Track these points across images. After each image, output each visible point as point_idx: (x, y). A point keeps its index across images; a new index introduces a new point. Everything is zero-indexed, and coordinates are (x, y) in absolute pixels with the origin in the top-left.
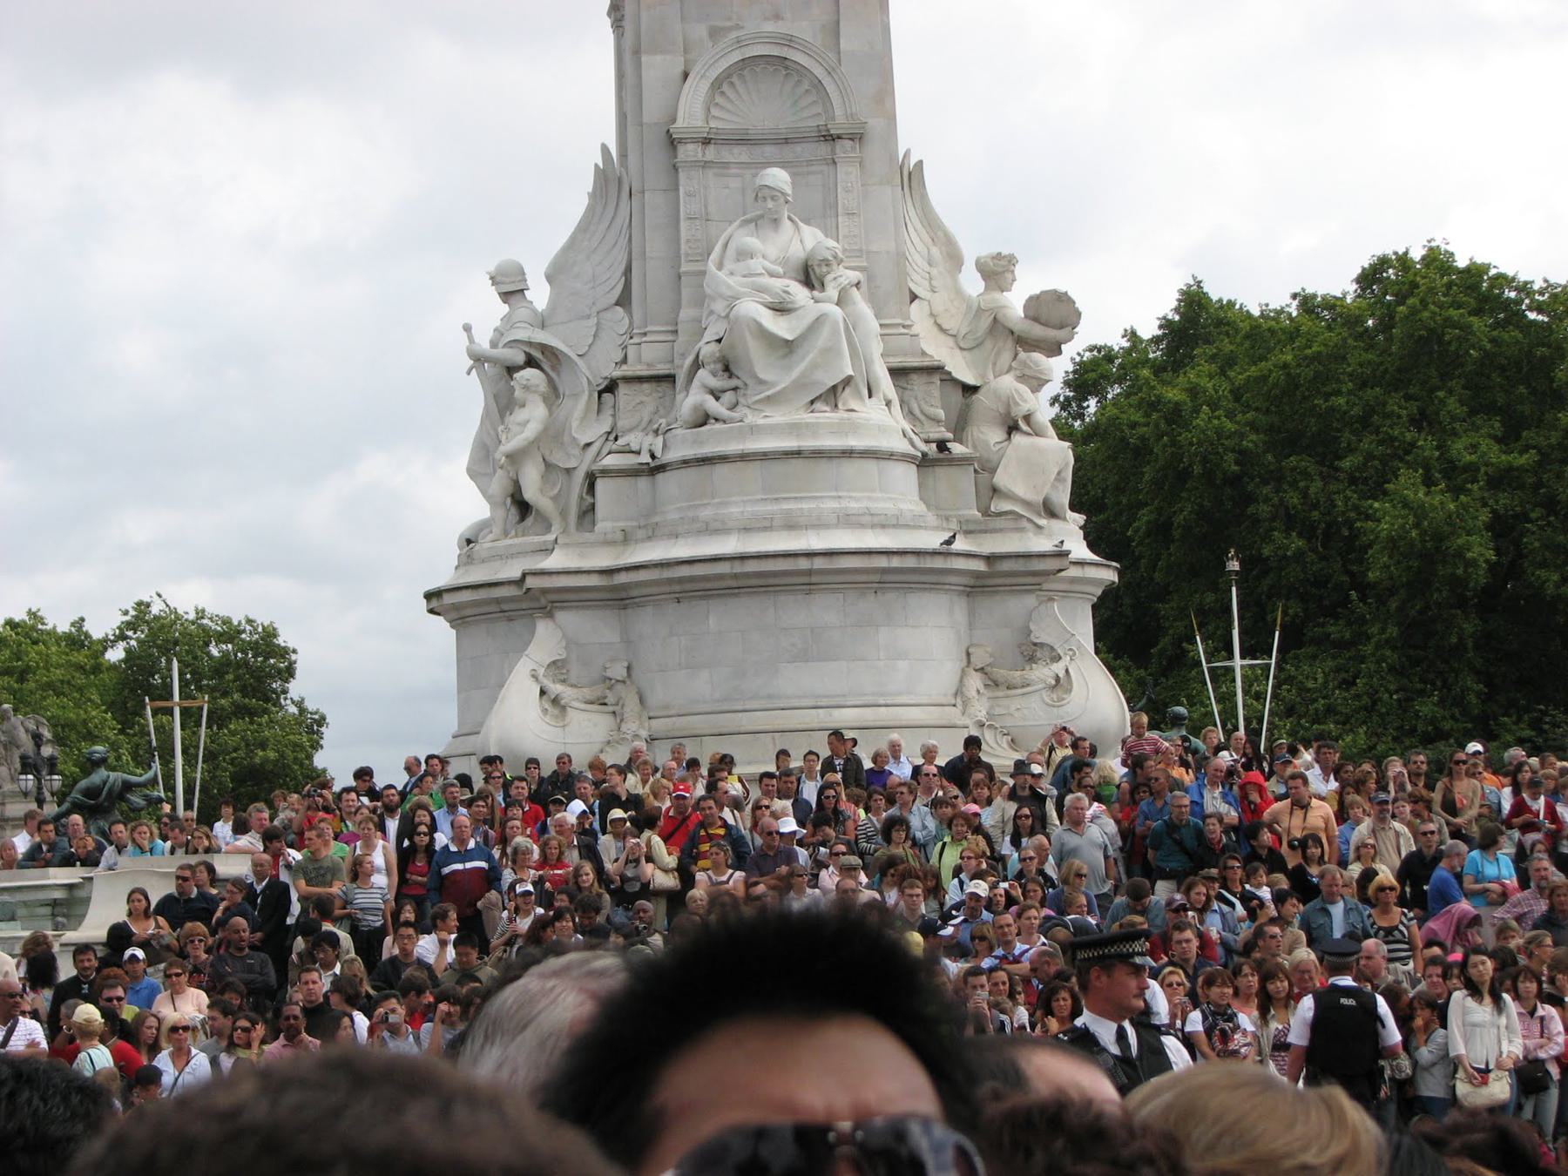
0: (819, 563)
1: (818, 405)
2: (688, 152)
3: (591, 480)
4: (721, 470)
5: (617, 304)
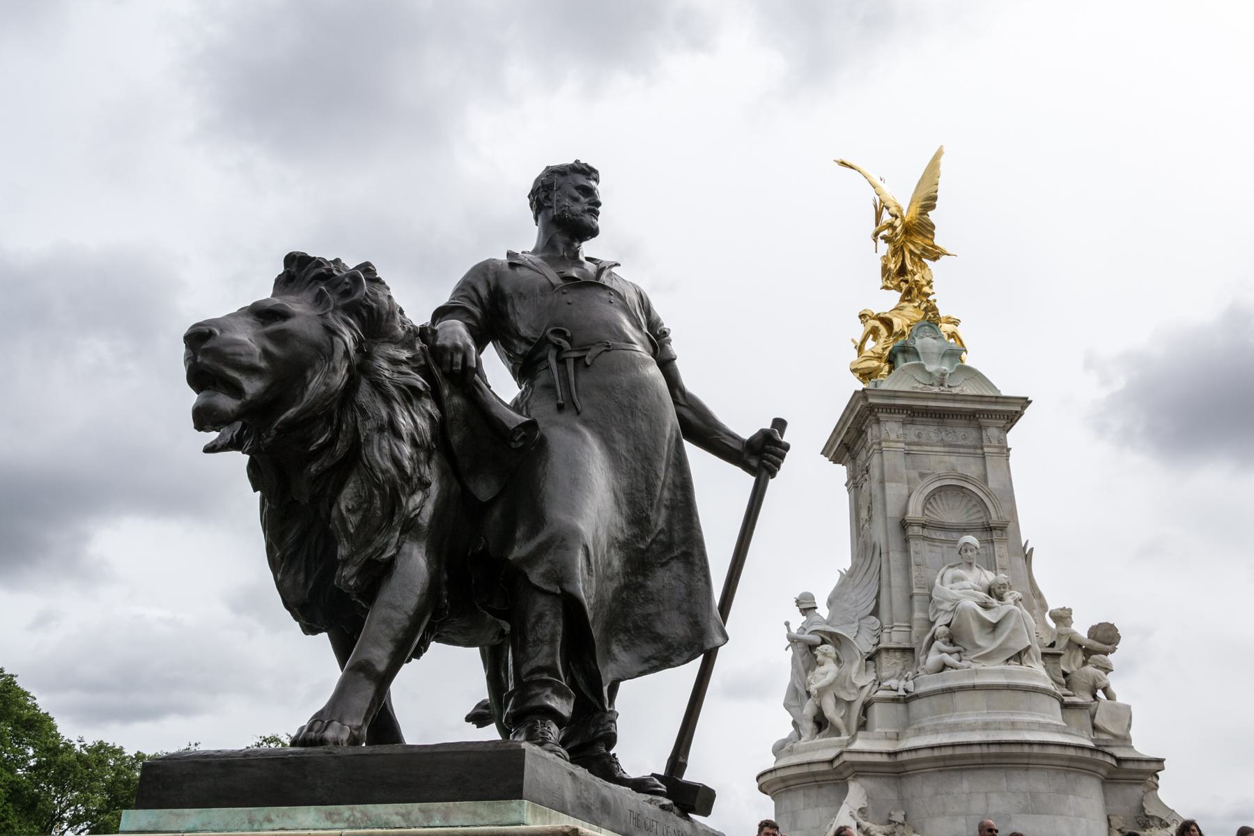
0: (1036, 750)
2: (916, 530)
3: (866, 707)
4: (959, 696)
5: (871, 614)
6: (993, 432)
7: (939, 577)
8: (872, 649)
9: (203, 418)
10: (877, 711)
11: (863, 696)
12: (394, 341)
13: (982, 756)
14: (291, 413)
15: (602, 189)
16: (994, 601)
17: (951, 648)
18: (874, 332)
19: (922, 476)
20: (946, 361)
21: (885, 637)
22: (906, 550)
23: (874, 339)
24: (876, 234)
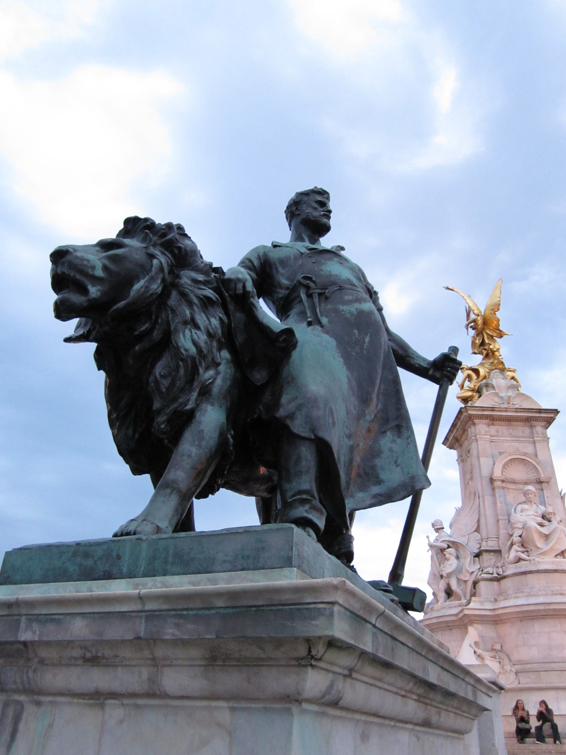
1: (558, 557)
3: (475, 583)
4: (530, 576)
5: (475, 531)
6: (539, 429)
7: (513, 510)
8: (476, 551)
9: (62, 311)
10: (482, 586)
11: (473, 578)
12: (197, 270)
13: (545, 610)
14: (122, 304)
15: (332, 205)
16: (546, 523)
17: (524, 550)
18: (469, 377)
19: (500, 453)
20: (510, 391)
21: (484, 543)
22: (494, 495)
23: (469, 381)
24: (467, 325)
